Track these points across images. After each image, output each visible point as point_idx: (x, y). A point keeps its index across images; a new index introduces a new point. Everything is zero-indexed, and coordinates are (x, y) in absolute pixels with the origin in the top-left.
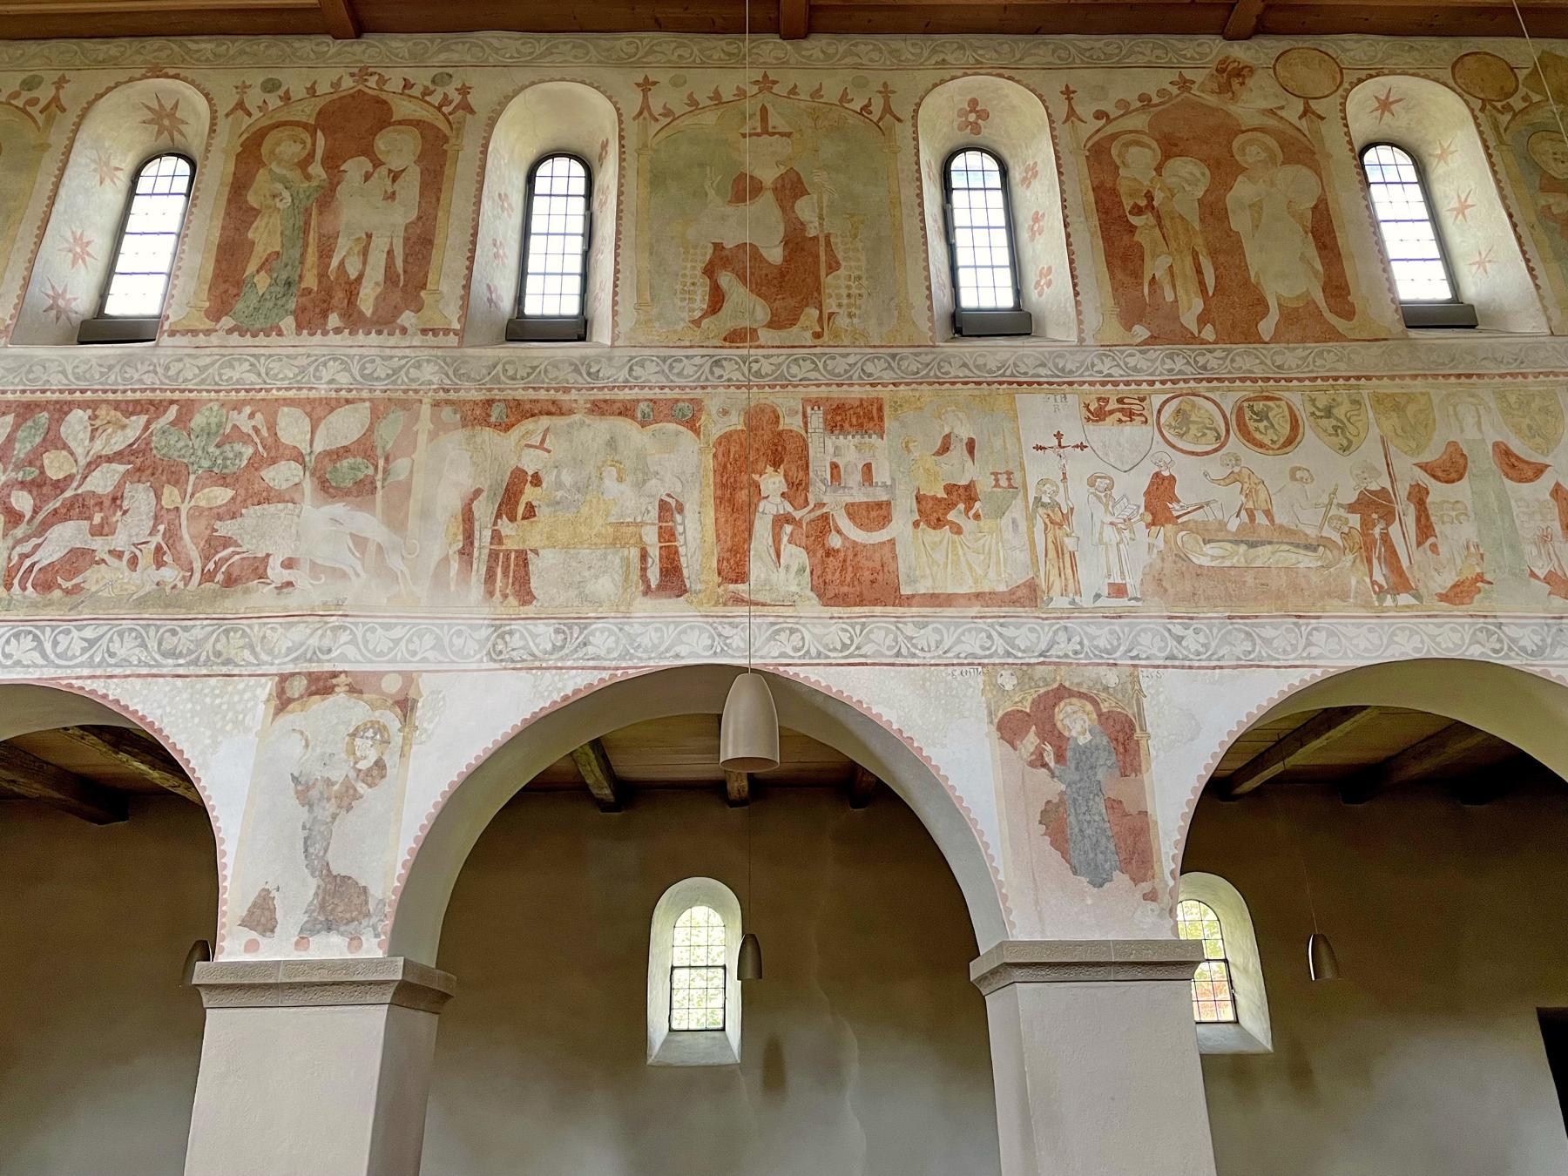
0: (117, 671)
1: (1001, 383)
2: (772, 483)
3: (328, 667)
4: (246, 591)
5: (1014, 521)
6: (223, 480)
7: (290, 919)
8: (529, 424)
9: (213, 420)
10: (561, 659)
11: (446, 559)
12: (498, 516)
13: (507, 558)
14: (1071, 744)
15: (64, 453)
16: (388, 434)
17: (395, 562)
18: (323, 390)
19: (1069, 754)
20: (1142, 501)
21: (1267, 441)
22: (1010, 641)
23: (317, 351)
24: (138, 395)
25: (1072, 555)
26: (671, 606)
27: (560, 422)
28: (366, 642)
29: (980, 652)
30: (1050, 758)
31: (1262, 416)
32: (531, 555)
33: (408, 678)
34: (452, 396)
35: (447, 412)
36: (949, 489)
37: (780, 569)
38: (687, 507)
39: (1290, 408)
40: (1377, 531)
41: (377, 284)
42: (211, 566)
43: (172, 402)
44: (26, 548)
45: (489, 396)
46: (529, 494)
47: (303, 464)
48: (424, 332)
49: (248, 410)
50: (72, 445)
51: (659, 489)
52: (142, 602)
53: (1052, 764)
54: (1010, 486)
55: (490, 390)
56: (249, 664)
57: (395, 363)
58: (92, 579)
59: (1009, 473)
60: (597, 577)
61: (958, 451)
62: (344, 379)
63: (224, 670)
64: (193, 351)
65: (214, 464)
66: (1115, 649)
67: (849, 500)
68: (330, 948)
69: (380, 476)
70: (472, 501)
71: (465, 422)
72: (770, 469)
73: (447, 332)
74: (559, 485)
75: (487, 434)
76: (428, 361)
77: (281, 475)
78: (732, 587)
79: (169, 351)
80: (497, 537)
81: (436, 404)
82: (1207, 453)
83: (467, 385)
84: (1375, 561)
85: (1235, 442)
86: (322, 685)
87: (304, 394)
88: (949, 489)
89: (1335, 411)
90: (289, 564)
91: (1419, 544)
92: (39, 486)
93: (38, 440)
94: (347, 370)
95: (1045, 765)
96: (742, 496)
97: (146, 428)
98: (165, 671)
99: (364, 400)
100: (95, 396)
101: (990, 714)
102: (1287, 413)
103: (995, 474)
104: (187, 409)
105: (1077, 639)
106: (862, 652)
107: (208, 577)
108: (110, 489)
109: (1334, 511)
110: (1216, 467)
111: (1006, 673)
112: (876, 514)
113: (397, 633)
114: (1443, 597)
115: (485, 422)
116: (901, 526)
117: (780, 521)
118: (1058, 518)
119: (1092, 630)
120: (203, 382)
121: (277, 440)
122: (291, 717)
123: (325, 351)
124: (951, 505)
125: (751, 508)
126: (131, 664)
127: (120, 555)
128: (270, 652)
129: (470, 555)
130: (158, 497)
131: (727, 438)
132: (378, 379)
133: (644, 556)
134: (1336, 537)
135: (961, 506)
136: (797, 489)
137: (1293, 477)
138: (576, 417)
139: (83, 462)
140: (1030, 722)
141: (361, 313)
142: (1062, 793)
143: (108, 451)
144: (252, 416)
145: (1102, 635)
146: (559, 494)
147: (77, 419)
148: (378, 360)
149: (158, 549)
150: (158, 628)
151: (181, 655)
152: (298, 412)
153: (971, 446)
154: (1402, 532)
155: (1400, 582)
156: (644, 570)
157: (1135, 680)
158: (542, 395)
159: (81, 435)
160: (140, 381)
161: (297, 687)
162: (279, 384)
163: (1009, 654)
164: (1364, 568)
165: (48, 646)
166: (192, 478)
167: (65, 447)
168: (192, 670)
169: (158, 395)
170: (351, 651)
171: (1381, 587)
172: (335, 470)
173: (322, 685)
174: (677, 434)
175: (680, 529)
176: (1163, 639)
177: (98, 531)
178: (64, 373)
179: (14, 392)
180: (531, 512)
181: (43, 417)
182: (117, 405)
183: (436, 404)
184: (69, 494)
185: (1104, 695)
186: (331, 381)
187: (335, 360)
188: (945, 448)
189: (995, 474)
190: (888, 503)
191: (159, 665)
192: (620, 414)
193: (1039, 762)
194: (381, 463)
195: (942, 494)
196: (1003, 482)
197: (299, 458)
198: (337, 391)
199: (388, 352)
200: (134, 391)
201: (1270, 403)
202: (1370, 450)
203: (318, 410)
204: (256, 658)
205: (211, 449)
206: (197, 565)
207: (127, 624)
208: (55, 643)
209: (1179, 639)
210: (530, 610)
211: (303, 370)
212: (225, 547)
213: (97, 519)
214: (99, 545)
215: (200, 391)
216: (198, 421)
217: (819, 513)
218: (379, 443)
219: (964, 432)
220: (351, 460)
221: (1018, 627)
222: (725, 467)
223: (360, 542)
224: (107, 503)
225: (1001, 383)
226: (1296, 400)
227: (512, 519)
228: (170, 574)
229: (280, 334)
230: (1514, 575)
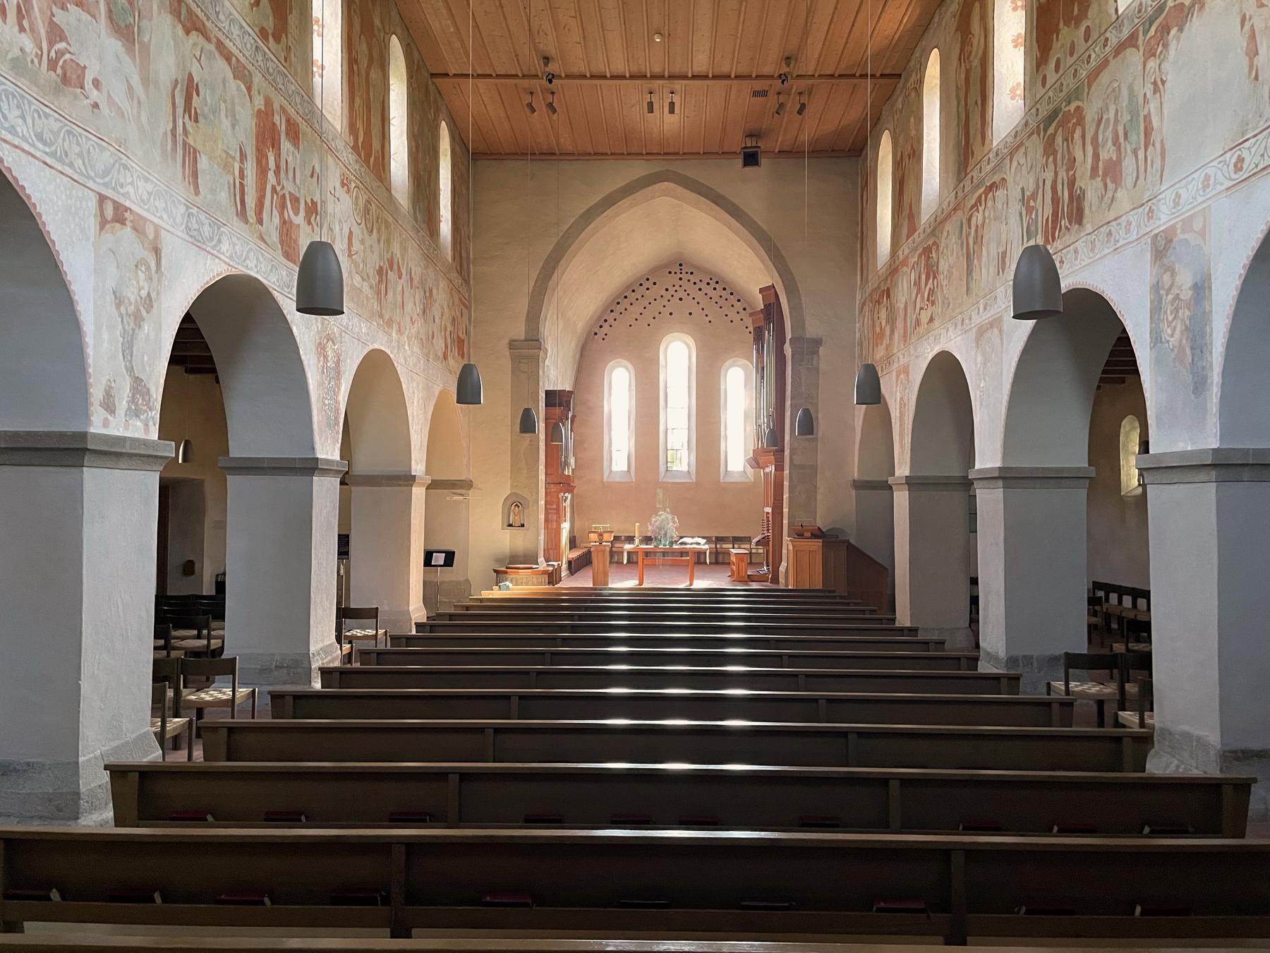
42: (53, 54)
98: (38, 154)
107: (52, 65)
131: (259, 111)
161: (109, 212)
210: (198, 200)
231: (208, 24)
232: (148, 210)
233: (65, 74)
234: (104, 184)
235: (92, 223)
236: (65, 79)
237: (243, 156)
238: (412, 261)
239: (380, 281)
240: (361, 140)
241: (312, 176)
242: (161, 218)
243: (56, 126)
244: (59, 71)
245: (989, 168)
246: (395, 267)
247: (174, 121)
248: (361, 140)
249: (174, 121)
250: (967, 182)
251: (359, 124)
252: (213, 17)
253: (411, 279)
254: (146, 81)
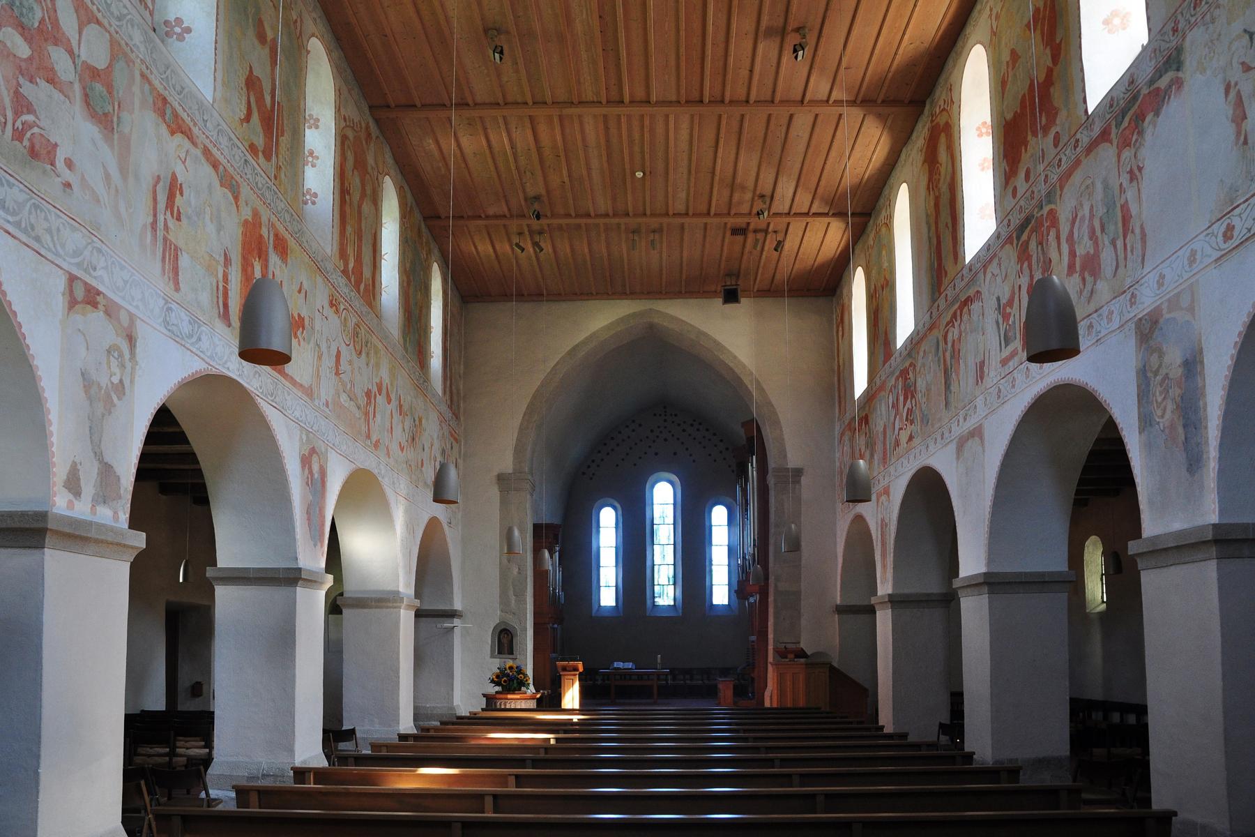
10: (192, 344)
42: (19, 124)
46: (179, 200)
107: (18, 135)
131: (246, 221)
132: (112, 14)
161: (80, 293)
172: (92, 89)
197: (71, 52)
231: (195, 130)
232: (123, 298)
234: (78, 265)
235: (60, 302)
236: (33, 153)
237: (227, 261)
238: (403, 386)
239: (369, 403)
240: (351, 265)
241: (300, 291)
242: (137, 307)
243: (22, 197)
244: (26, 143)
245: (963, 284)
246: (384, 391)
247: (155, 215)
248: (351, 265)
249: (155, 215)
250: (941, 302)
251: (350, 251)
252: (200, 123)
253: (401, 406)
254: (123, 171)
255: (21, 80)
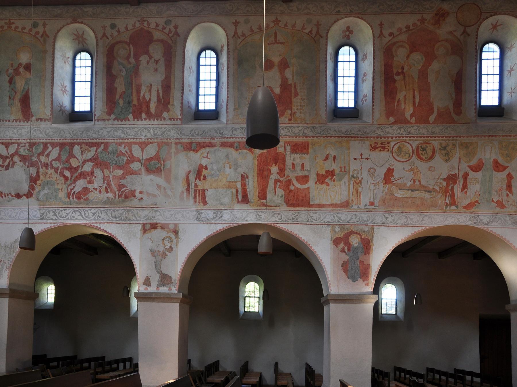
0: (102, 222)
1: (346, 137)
2: (274, 169)
3: (155, 222)
4: (131, 200)
5: (345, 182)
6: (120, 168)
7: (154, 283)
8: (203, 150)
9: (114, 149)
10: (216, 221)
11: (183, 192)
12: (196, 179)
13: (199, 192)
14: (352, 247)
15: (75, 159)
16: (163, 154)
17: (169, 192)
18: (143, 139)
19: (351, 249)
20: (383, 176)
21: (424, 158)
22: (339, 218)
23: (141, 126)
24: (92, 141)
25: (360, 193)
26: (245, 207)
27: (212, 149)
28: (164, 215)
29: (330, 221)
30: (346, 250)
31: (424, 149)
32: (206, 191)
33: (176, 225)
34: (180, 141)
35: (179, 146)
36: (327, 172)
37: (275, 195)
38: (249, 176)
39: (433, 147)
40: (450, 187)
41: (155, 102)
42: (121, 193)
43: (102, 143)
44: (71, 187)
45: (191, 141)
46: (204, 172)
47: (141, 163)
48: (170, 119)
49: (123, 146)
50: (77, 156)
51: (241, 171)
52: (105, 203)
53: (346, 251)
54: (345, 171)
55: (191, 139)
56: (134, 220)
57: (163, 130)
58: (91, 196)
59: (345, 167)
60: (224, 197)
61: (331, 159)
62: (149, 135)
63: (129, 222)
64: (105, 126)
65: (117, 163)
66: (368, 221)
67: (297, 175)
68: (164, 290)
69: (162, 166)
70: (188, 174)
71: (185, 150)
72: (274, 165)
73: (177, 119)
74: (213, 170)
75: (191, 154)
76: (173, 129)
77: (135, 166)
78: (262, 201)
79: (99, 126)
80: (196, 185)
81: (176, 144)
82: (405, 161)
83: (184, 137)
84: (447, 196)
85: (414, 158)
86: (154, 226)
87: (138, 140)
88: (327, 172)
89: (447, 148)
90: (141, 192)
91: (462, 191)
92: (70, 169)
93: (67, 155)
94: (149, 132)
95: (344, 252)
96: (266, 173)
97: (96, 151)
98: (114, 222)
99: (155, 142)
100: (81, 141)
101: (332, 238)
102: (432, 149)
103: (341, 167)
104: (107, 145)
105: (358, 218)
106: (298, 220)
107: (120, 196)
108: (90, 170)
109: (439, 180)
110: (407, 166)
111: (337, 227)
112: (304, 179)
113: (172, 213)
114: (464, 207)
115: (190, 149)
116: (311, 183)
117: (276, 181)
118: (358, 181)
119: (363, 215)
120: (109, 136)
121: (133, 155)
122: (147, 234)
123: (142, 126)
124: (326, 177)
125: (268, 176)
126: (105, 220)
127: (96, 189)
128: (140, 217)
129: (189, 190)
130: (103, 173)
132: (159, 135)
133: (237, 191)
134: (438, 189)
135: (330, 177)
136: (281, 171)
137: (429, 170)
138: (217, 148)
139: (81, 162)
140: (341, 241)
141: (151, 113)
142: (348, 259)
143: (87, 158)
144: (125, 147)
145: (365, 216)
146: (213, 172)
147: (77, 148)
148: (158, 129)
149: (106, 188)
150: (110, 210)
151: (117, 218)
152: (137, 146)
153: (334, 158)
154: (457, 188)
155: (453, 203)
156: (237, 195)
157: (372, 229)
158: (206, 140)
159: (79, 154)
160: (92, 136)
161: (148, 227)
162: (131, 137)
163: (338, 221)
164: (443, 198)
165: (83, 214)
166: (111, 167)
167: (75, 157)
168: (121, 222)
169: (98, 141)
170: (160, 217)
171: (447, 204)
173: (154, 226)
174: (247, 153)
175: (247, 183)
176: (382, 218)
177: (90, 182)
178: (70, 133)
179: (57, 140)
180: (205, 178)
181: (67, 147)
182: (87, 144)
183: (176, 144)
184: (79, 171)
185: (363, 233)
186: (145, 136)
187: (146, 129)
188: (326, 159)
189: (341, 167)
190: (308, 176)
191: (112, 220)
192: (230, 147)
193: (343, 251)
194: (162, 162)
195: (324, 173)
196: (343, 170)
197: (139, 161)
198: (148, 139)
199: (161, 126)
200: (91, 139)
201: (428, 145)
202: (455, 162)
203: (143, 145)
204: (136, 218)
205: (115, 158)
206: (117, 193)
207: (102, 209)
208: (85, 214)
209: (387, 218)
211: (137, 133)
212: (123, 188)
213: (88, 179)
214: (90, 186)
215: (109, 139)
216: (110, 149)
217: (287, 179)
218: (161, 156)
219: (333, 153)
220: (154, 162)
221: (342, 214)
222: (260, 164)
223: (159, 187)
224: (90, 174)
225: (346, 137)
226: (436, 144)
227: (200, 180)
228: (110, 195)
229: (129, 120)
230: (487, 201)
233: (126, 195)
255: (120, 181)
